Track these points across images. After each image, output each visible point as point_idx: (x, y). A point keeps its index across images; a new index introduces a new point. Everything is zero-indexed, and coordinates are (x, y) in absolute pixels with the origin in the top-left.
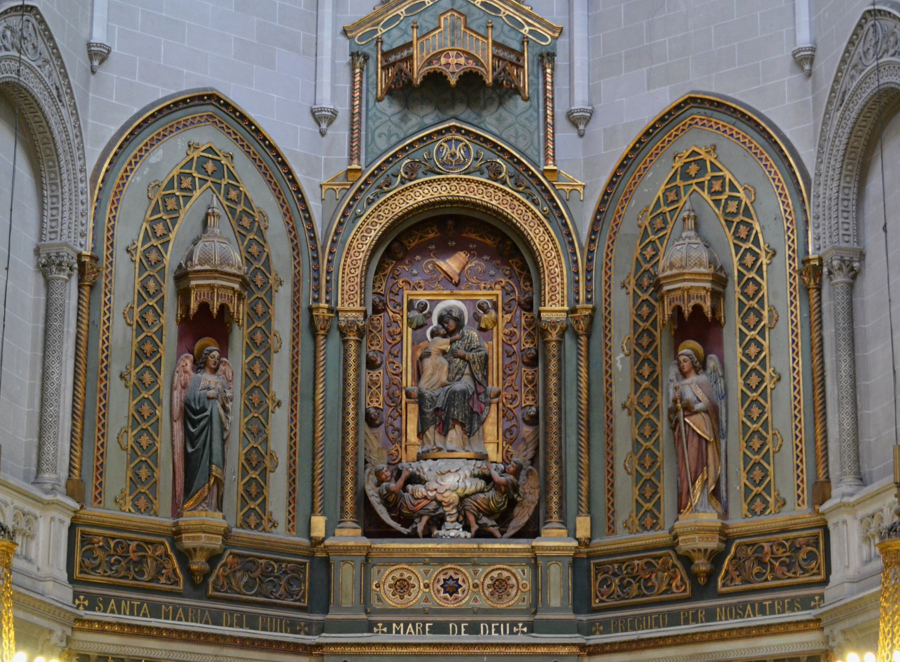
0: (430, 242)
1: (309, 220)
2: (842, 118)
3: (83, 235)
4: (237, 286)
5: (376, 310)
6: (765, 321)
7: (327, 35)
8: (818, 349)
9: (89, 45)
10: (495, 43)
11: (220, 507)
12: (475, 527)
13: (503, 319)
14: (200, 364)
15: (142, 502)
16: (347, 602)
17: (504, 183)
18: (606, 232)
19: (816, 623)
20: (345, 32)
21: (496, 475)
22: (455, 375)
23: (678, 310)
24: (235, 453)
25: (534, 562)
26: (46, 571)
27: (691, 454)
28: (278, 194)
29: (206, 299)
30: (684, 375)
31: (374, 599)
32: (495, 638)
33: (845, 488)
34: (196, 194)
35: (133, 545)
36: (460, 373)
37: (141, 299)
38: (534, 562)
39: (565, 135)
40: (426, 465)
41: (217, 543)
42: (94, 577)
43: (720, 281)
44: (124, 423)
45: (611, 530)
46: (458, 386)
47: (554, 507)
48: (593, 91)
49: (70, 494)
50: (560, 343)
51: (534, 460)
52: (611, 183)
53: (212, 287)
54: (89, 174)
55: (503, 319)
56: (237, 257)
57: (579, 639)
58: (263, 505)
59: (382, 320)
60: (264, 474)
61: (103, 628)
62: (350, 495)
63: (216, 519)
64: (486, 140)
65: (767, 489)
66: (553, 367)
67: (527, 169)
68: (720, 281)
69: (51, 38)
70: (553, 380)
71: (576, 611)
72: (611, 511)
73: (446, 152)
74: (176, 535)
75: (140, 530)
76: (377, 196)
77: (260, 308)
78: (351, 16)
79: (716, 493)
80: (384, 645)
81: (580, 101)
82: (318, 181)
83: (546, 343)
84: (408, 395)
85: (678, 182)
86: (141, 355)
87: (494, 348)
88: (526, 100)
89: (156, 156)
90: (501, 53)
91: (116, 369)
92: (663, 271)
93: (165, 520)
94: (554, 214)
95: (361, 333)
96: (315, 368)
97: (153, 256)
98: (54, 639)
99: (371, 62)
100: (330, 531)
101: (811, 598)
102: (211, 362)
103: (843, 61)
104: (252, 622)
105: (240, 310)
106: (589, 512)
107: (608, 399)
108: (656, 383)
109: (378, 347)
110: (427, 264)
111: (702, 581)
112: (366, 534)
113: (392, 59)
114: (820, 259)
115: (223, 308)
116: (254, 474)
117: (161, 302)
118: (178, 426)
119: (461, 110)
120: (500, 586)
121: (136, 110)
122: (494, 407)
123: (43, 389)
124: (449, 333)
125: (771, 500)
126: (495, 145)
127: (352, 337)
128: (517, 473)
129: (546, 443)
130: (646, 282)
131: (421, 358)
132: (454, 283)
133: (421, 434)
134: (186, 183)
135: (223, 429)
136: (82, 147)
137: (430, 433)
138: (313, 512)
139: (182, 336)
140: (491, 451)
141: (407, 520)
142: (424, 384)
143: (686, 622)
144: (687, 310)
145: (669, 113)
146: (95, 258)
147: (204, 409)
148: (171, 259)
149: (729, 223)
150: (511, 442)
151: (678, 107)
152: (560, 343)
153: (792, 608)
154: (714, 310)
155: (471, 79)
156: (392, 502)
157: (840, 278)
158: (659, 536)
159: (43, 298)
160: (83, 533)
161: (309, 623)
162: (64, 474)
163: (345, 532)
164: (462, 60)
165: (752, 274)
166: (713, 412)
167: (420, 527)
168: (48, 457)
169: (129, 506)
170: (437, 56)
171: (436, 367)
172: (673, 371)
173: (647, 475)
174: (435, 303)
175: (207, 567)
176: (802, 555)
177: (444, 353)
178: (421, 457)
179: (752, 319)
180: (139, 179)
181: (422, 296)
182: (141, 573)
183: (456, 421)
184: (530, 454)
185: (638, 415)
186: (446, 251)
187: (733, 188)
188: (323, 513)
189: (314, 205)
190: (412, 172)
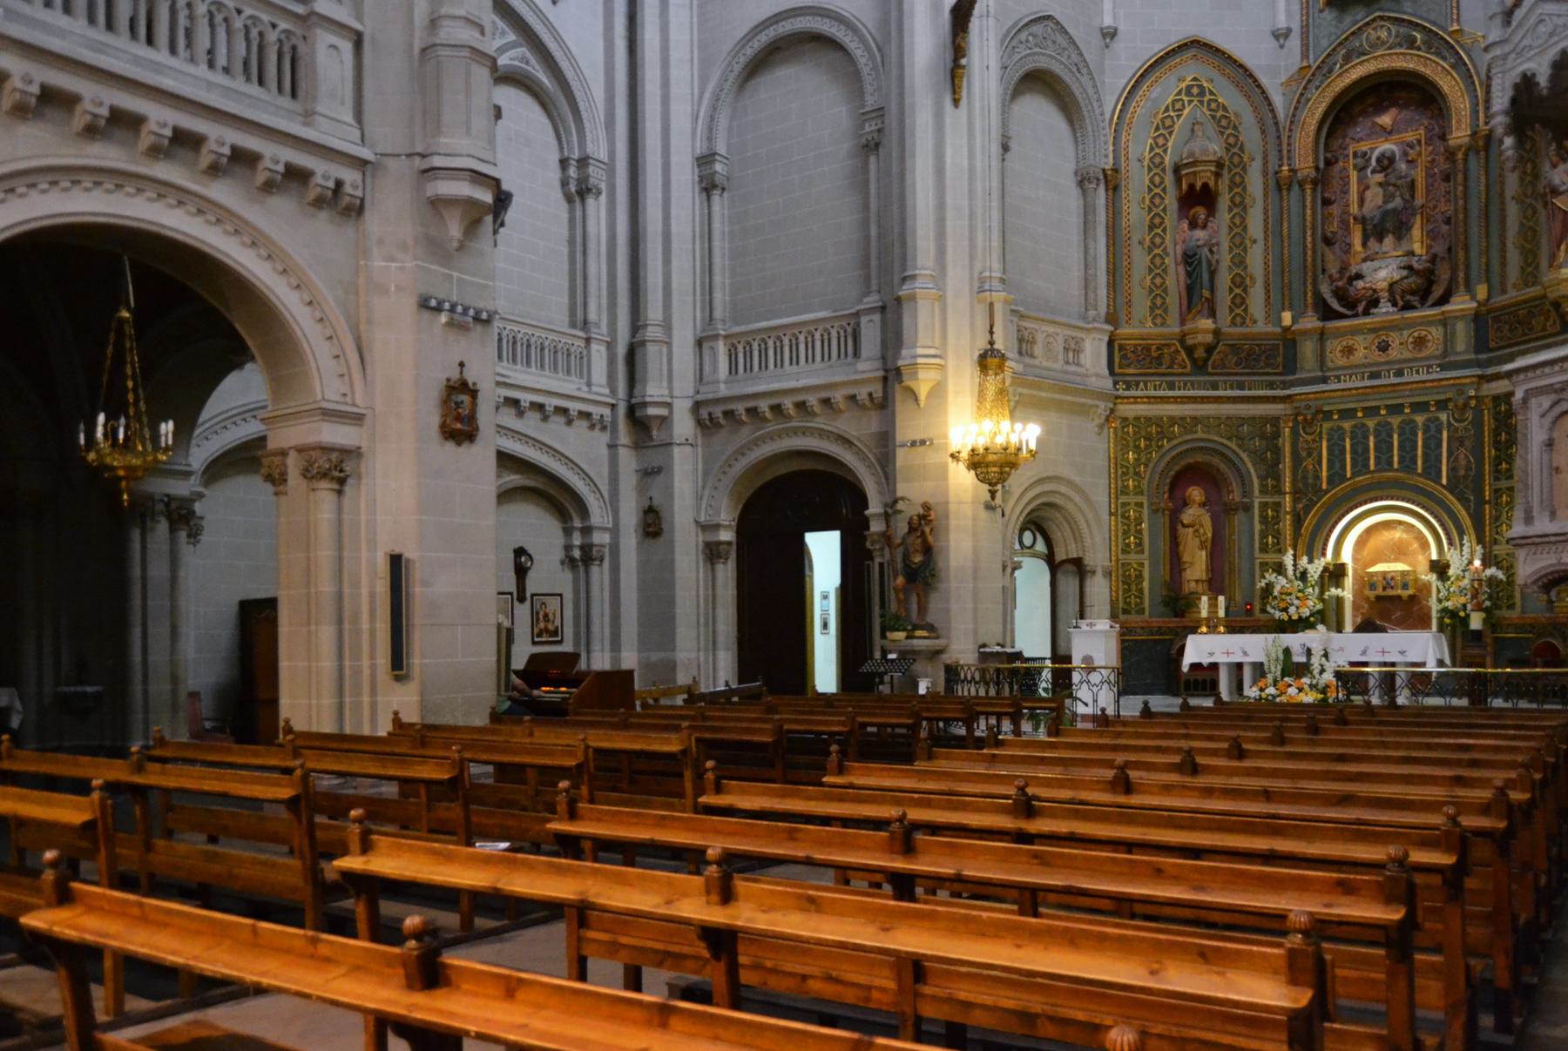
4: (1213, 169)
12: (1401, 303)
14: (1193, 225)
17: (1419, 49)
22: (1388, 198)
24: (1224, 279)
25: (1444, 322)
32: (1416, 378)
36: (1393, 196)
38: (1444, 322)
40: (1366, 267)
46: (1390, 206)
47: (1461, 281)
57: (1479, 372)
58: (1245, 310)
62: (1310, 294)
64: (1403, 20)
67: (1437, 34)
84: (1355, 219)
87: (1419, 175)
100: (1294, 320)
104: (1241, 386)
116: (1237, 291)
118: (1181, 269)
120: (1420, 342)
122: (1418, 218)
126: (1410, 22)
127: (1308, 187)
131: (1364, 191)
132: (1387, 132)
133: (1364, 245)
138: (1283, 310)
142: (1366, 209)
161: (1283, 383)
167: (1360, 309)
174: (1372, 150)
177: (1380, 184)
183: (1388, 231)
186: (1380, 109)
188: (1291, 309)
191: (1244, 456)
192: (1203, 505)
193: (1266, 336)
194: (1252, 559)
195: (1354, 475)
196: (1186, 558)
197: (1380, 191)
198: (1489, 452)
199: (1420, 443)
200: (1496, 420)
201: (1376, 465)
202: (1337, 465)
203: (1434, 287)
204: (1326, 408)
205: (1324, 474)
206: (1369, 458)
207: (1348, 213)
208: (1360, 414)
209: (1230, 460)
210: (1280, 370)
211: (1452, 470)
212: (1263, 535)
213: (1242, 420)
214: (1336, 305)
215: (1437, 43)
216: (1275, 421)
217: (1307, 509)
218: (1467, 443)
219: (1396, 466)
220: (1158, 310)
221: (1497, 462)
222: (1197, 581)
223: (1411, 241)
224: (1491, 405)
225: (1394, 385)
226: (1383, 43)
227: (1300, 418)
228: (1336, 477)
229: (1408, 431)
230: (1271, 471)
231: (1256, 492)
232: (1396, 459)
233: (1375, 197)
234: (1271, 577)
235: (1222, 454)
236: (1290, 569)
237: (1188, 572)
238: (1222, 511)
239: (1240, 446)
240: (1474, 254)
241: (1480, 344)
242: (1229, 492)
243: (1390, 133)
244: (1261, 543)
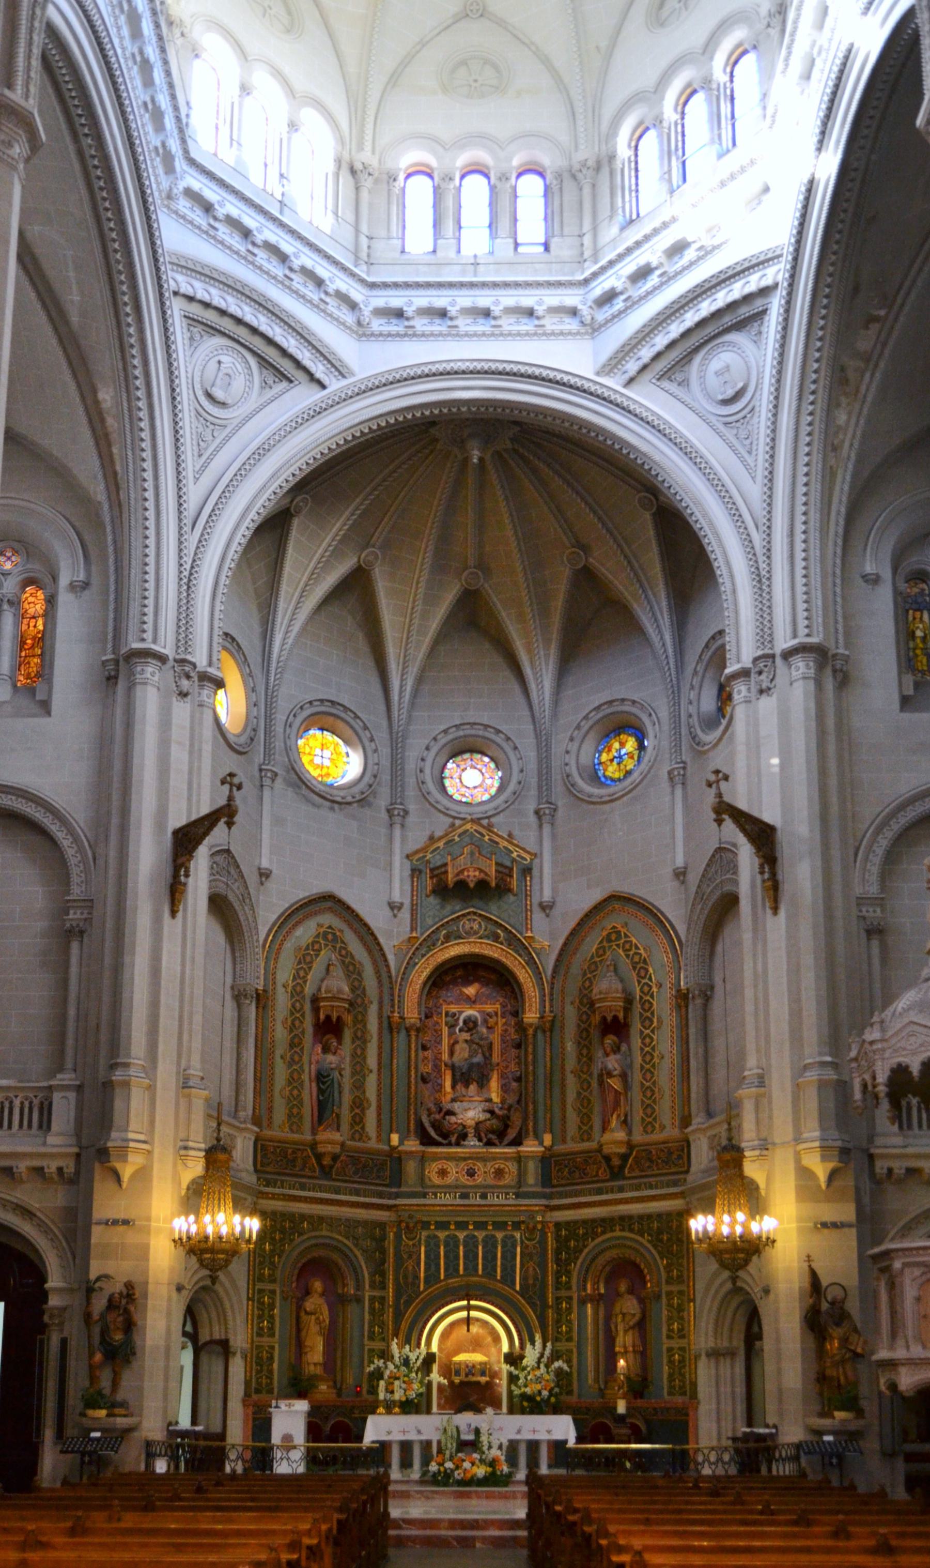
0: (460, 977)
1: (388, 966)
2: (702, 909)
3: (258, 978)
5: (427, 1017)
6: (655, 1024)
7: (397, 859)
8: (684, 1041)
9: (259, 869)
10: (497, 864)
11: (338, 1130)
12: (485, 1140)
13: (501, 1021)
14: (326, 1050)
15: (295, 1127)
16: (410, 1182)
18: (562, 972)
19: (682, 1195)
20: (408, 857)
21: (497, 1110)
22: (472, 1054)
23: (604, 1019)
24: (347, 1098)
25: (519, 1159)
26: (242, 1166)
27: (610, 1098)
28: (369, 951)
29: (329, 1013)
30: (607, 1055)
31: (427, 1181)
32: (496, 1201)
33: (699, 1120)
34: (323, 952)
35: (290, 1151)
36: (476, 1052)
37: (292, 1014)
38: (519, 1159)
39: (538, 916)
40: (456, 1106)
41: (337, 1149)
42: (268, 1169)
43: (629, 1001)
44: (283, 1083)
45: (564, 1141)
47: (531, 1129)
48: (554, 890)
49: (254, 1124)
50: (535, 1035)
51: (519, 1102)
52: (565, 944)
53: (333, 1007)
54: (261, 942)
55: (501, 1021)
56: (346, 989)
57: (544, 1202)
58: (363, 1128)
59: (430, 1022)
60: (363, 1111)
61: (274, 1197)
62: (412, 1122)
63: (337, 1137)
65: (655, 1119)
66: (530, 1050)
68: (629, 1001)
69: (238, 867)
70: (530, 1057)
71: (543, 1186)
72: (564, 1131)
73: (467, 926)
74: (314, 1145)
75: (295, 1143)
76: (428, 952)
77: (360, 1017)
78: (412, 846)
79: (625, 1122)
80: (433, 1205)
81: (547, 896)
82: (392, 944)
83: (526, 1036)
85: (605, 944)
86: (292, 1045)
87: (496, 1038)
88: (515, 895)
89: (299, 932)
90: (500, 869)
91: (278, 1053)
92: (595, 994)
93: (308, 1137)
94: (531, 962)
95: (418, 1030)
96: (392, 1051)
97: (298, 989)
98: (247, 1203)
99: (423, 875)
100: (401, 1142)
101: (679, 1180)
102: (333, 1049)
103: (703, 876)
104: (357, 1193)
105: (348, 1019)
106: (551, 1132)
107: (563, 1067)
108: (590, 1059)
109: (427, 1038)
110: (456, 991)
111: (616, 1170)
112: (422, 1144)
113: (436, 872)
114: (688, 989)
115: (339, 1018)
116: (357, 1111)
117: (303, 1015)
118: (314, 1085)
119: (476, 902)
120: (499, 1173)
121: (287, 905)
123: (238, 1065)
124: (469, 1030)
125: (657, 1126)
126: (496, 922)
127: (413, 1033)
128: (509, 1109)
129: (526, 1094)
130: (585, 1001)
131: (453, 1044)
132: (471, 1001)
134: (316, 947)
135: (340, 1086)
136: (256, 928)
137: (459, 1086)
138: (391, 1131)
139: (315, 1034)
140: (495, 1097)
141: (445, 1136)
142: (456, 1059)
143: (607, 1193)
144: (609, 1019)
145: (600, 904)
146: (265, 991)
147: (328, 1076)
148: (309, 990)
149: (634, 968)
150: (505, 1092)
151: (605, 900)
152: (535, 1035)
153: (668, 1186)
154: (625, 1018)
155: (482, 885)
156: (436, 1126)
157: (699, 1001)
158: (593, 1145)
159: (236, 1014)
160: (262, 1145)
162: (250, 1112)
163: (411, 1143)
164: (477, 873)
165: (648, 998)
166: (624, 1076)
167: (453, 1139)
168: (241, 1103)
169: (287, 1129)
170: (462, 871)
171: (462, 1049)
172: (600, 1053)
173: (584, 1111)
174: (461, 1013)
175: (331, 1163)
176: (675, 1156)
177: (466, 1041)
178: (454, 1100)
179: (647, 1023)
180: (289, 945)
181: (453, 1009)
182: (294, 1166)
184: (517, 1098)
185: (580, 1077)
186: (468, 983)
187: (637, 948)
188: (397, 1132)
189: (391, 958)
190: (447, 938)
191: (358, 1253)
192: (323, 1294)
193: (379, 1152)
194: (362, 1346)
195: (447, 1277)
196: (308, 1343)
197: (465, 1045)
198: (551, 1267)
199: (499, 1255)
200: (557, 1241)
201: (465, 1269)
202: (433, 1268)
203: (509, 1130)
204: (425, 1219)
205: (422, 1275)
206: (458, 1265)
207: (440, 1060)
208: (452, 1227)
209: (347, 1256)
210: (388, 1182)
211: (524, 1279)
212: (371, 1326)
213: (358, 1223)
214: (432, 1133)
215: (513, 941)
216: (382, 1225)
217: (408, 1303)
218: (535, 1258)
219: (480, 1272)
220: (294, 1118)
221: (558, 1275)
222: (315, 1364)
223: (489, 1090)
224: (552, 1229)
225: (479, 1206)
226: (476, 933)
227: (403, 1225)
228: (431, 1278)
229: (490, 1243)
230: (379, 1270)
231: (367, 1287)
232: (480, 1267)
233: (462, 1053)
234: (381, 1363)
235: (340, 1251)
236: (397, 1355)
237: (309, 1356)
238: (337, 1301)
239: (356, 1245)
240: (541, 1109)
241: (546, 1179)
242: (344, 1285)
243: (474, 1002)
244: (369, 1331)
